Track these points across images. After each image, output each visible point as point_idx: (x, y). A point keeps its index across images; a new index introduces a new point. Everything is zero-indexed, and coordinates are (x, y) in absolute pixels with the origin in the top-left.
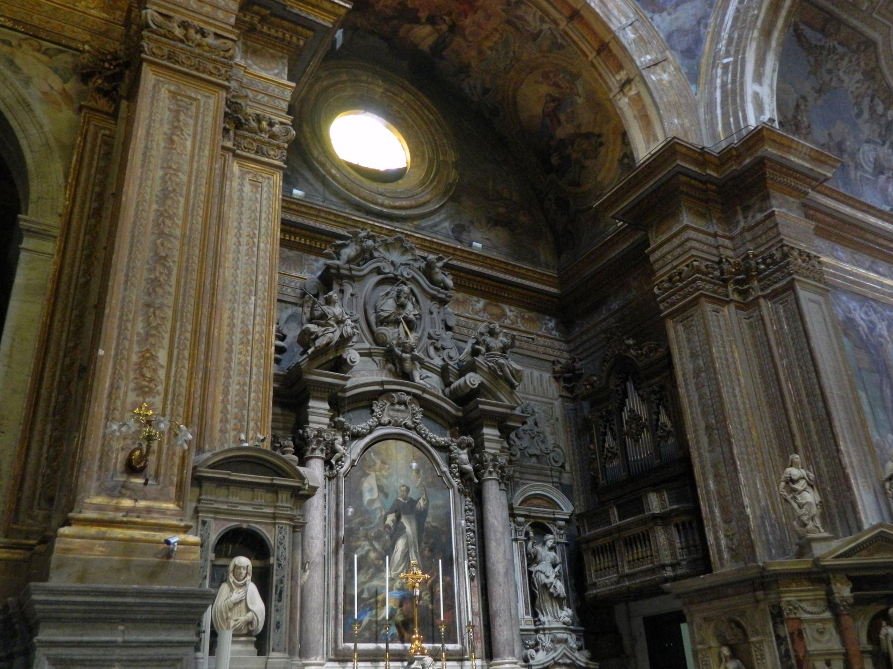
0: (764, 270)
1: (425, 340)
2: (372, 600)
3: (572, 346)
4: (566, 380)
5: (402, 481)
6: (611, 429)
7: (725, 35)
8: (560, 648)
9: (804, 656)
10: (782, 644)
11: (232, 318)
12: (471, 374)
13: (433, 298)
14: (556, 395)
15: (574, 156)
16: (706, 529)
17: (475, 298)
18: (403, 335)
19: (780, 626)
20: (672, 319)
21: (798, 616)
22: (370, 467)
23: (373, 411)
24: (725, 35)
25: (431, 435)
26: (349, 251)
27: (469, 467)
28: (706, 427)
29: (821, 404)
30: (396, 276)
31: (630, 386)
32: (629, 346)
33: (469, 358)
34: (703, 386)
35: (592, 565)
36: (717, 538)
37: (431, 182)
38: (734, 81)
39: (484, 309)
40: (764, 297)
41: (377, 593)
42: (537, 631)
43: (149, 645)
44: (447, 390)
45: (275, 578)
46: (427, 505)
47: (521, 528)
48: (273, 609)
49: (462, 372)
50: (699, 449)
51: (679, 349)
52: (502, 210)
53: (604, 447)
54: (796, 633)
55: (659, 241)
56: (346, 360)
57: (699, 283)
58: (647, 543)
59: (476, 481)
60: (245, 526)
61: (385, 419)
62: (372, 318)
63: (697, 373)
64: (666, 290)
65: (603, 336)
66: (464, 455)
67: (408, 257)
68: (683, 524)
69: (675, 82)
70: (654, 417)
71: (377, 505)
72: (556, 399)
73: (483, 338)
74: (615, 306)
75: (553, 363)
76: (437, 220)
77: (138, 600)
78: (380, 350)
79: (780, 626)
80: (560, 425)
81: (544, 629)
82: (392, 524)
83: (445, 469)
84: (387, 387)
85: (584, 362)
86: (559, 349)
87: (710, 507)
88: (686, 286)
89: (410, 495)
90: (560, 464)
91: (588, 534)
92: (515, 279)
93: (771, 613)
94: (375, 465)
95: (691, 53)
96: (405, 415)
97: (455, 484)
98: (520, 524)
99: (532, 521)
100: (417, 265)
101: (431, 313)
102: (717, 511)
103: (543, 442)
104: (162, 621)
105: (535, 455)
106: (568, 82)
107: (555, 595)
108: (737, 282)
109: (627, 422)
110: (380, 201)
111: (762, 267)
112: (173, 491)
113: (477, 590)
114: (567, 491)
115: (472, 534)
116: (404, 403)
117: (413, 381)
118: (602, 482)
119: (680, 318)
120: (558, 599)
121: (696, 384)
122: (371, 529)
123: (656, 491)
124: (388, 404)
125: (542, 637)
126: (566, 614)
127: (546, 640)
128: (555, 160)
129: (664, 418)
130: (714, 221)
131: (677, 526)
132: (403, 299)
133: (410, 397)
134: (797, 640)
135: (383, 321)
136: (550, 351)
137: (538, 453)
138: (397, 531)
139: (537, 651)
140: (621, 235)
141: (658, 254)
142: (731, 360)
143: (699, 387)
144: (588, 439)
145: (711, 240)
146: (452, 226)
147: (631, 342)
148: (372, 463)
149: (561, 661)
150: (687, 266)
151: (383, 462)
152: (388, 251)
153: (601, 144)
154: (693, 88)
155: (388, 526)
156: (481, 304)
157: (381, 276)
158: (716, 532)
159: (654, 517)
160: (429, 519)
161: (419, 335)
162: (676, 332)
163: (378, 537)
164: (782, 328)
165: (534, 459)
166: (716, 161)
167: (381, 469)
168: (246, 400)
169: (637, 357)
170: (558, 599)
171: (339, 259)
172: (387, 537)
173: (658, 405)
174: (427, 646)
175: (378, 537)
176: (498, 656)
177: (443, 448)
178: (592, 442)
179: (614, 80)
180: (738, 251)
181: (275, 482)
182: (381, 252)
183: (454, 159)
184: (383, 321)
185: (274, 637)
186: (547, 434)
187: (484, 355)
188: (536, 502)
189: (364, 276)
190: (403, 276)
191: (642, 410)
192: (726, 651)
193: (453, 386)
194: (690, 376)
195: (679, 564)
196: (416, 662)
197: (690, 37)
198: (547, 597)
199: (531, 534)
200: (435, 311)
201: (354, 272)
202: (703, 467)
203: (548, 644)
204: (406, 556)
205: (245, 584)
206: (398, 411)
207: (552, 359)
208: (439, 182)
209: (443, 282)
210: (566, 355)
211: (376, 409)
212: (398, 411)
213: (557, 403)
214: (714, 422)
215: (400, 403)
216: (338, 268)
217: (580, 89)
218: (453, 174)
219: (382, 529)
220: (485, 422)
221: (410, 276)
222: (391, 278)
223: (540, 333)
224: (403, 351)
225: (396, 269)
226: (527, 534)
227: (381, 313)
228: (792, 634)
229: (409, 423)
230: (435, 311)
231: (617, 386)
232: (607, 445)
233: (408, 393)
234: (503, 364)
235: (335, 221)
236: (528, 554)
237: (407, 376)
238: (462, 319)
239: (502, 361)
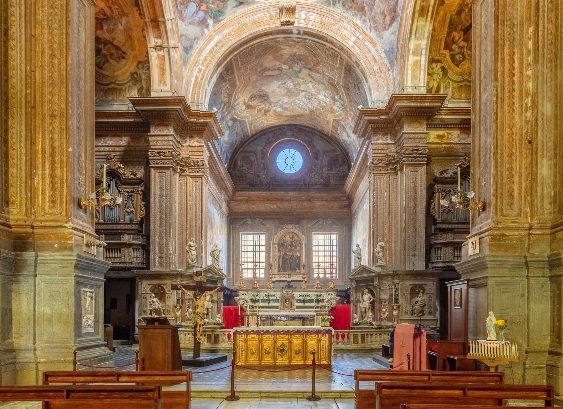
7: (205, 54)
24: (205, 54)
29: (200, 222)
32: (120, 167)
38: (202, 79)
64: (155, 156)
69: (178, 61)
70: (125, 202)
95: (187, 50)
106: (119, 13)
108: (182, 166)
154: (184, 68)
169: (123, 174)
173: (128, 198)
179: (153, 41)
197: (189, 43)
217: (124, 22)
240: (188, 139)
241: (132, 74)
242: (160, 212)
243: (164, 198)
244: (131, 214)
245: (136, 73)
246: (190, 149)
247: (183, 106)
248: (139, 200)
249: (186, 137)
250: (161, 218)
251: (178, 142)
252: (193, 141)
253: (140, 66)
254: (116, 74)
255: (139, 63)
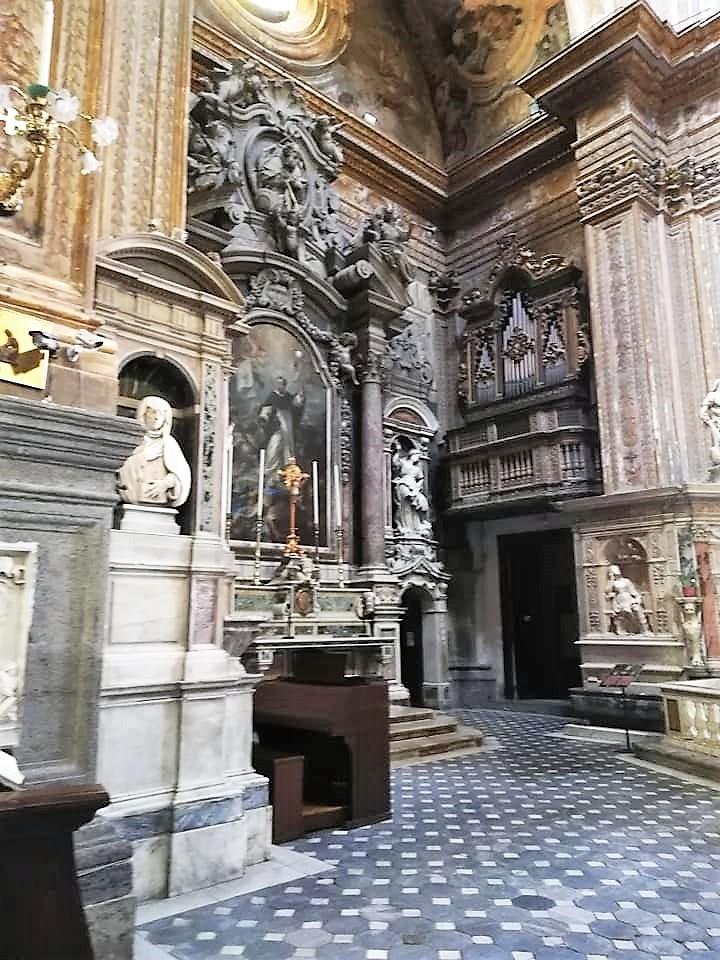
0: (701, 182)
1: (309, 216)
2: (243, 496)
3: (450, 259)
4: (441, 295)
5: (279, 373)
6: (489, 349)
8: (418, 559)
9: (708, 579)
10: (686, 566)
11: (126, 58)
12: (363, 262)
13: (321, 169)
14: (430, 310)
15: (483, 34)
16: (603, 451)
17: (359, 185)
18: (288, 203)
19: (687, 548)
20: (593, 225)
21: (706, 540)
22: (246, 351)
23: (250, 288)
25: (311, 326)
26: (231, 86)
27: (351, 367)
28: (619, 346)
30: (283, 131)
31: (517, 303)
33: (360, 245)
34: (622, 301)
35: (459, 479)
36: (614, 461)
37: (320, 33)
39: (367, 200)
40: (696, 212)
41: (247, 489)
42: (396, 541)
43: (39, 496)
44: (331, 279)
45: (202, 435)
46: (304, 402)
47: (388, 440)
48: (200, 474)
49: (351, 260)
50: (606, 369)
51: (598, 259)
52: (392, 89)
53: (477, 367)
54: (703, 556)
55: (590, 134)
56: (227, 215)
57: (635, 184)
58: (528, 463)
59: (357, 383)
60: (160, 355)
61: (264, 299)
62: (253, 176)
63: (616, 287)
65: (496, 246)
66: (345, 353)
67: (295, 112)
68: (570, 445)
70: (544, 337)
71: (252, 394)
72: (429, 314)
73: (379, 221)
74: (508, 217)
75: (430, 273)
76: (324, 81)
77: (20, 422)
78: (261, 217)
79: (687, 548)
80: (430, 341)
81: (404, 540)
82: (266, 417)
83: (325, 366)
84: (269, 261)
85: (460, 277)
86: (437, 260)
87: (611, 429)
88: (619, 187)
89: (287, 389)
90: (428, 381)
91: (458, 451)
92: (404, 170)
93: (679, 536)
94: (251, 349)
96: (286, 298)
97: (335, 386)
98: (387, 436)
99: (399, 434)
100: (307, 123)
101: (317, 187)
102: (618, 433)
103: (414, 355)
104: (60, 462)
105: (407, 368)
107: (418, 508)
109: (509, 341)
110: (262, 39)
111: (700, 177)
112: (66, 263)
113: (349, 497)
114: (433, 407)
115: (347, 439)
116: (286, 284)
117: (297, 259)
118: (470, 402)
119: (604, 224)
120: (421, 513)
121: (613, 299)
122: (244, 420)
123: (545, 411)
124: (268, 282)
125: (401, 546)
126: (425, 527)
127: (404, 550)
128: (458, 38)
129: (554, 338)
130: (653, 120)
131: (563, 446)
132: (291, 159)
133: (292, 278)
134: (703, 563)
135: (267, 182)
136: (427, 260)
137: (410, 366)
138: (272, 426)
139: (396, 559)
140: (534, 129)
141: (587, 149)
142: (654, 277)
143: (615, 302)
144: (458, 359)
145: (648, 139)
146: (339, 94)
147: (528, 254)
148: (247, 347)
149: (418, 571)
150: (624, 164)
151: (260, 349)
152: (274, 97)
153: (519, 22)
155: (263, 419)
156: (365, 193)
157: (265, 128)
158: (613, 455)
159: (542, 436)
160: (306, 417)
161: (305, 207)
162: (596, 241)
163: (252, 430)
164: (711, 247)
165: (404, 372)
166: (673, 41)
167: (256, 356)
168: (149, 186)
169: (533, 271)
170: (421, 513)
171: (216, 93)
172: (262, 431)
173: (550, 324)
174: (304, 548)
175: (252, 430)
176: (368, 562)
177: (326, 344)
178: (464, 361)
180: (672, 158)
181: (203, 299)
182: (266, 96)
183: (346, 12)
184: (267, 182)
185: (201, 512)
186: (419, 349)
187: (377, 241)
188: (404, 416)
189: (246, 121)
190: (289, 133)
191: (530, 331)
192: (615, 569)
193: (338, 275)
194: (607, 289)
195: (560, 484)
196: (291, 563)
198: (408, 509)
199: (399, 447)
200: (322, 185)
201: (234, 114)
202: (608, 387)
203: (407, 554)
204: (280, 453)
205: (161, 436)
206: (279, 292)
207: (430, 269)
208: (329, 33)
209: (333, 152)
210: (443, 269)
211: (254, 285)
212: (279, 292)
213: (431, 317)
214: (630, 340)
215: (280, 283)
216: (215, 103)
218: (345, 28)
219: (255, 421)
220: (372, 320)
221: (296, 136)
222: (275, 132)
223: (420, 238)
224: (289, 223)
225: (283, 123)
226: (393, 446)
227: (266, 172)
228: (699, 557)
229: (289, 309)
230: (322, 185)
231: (503, 303)
232: (481, 366)
233: (292, 273)
234: (398, 254)
235: (213, 45)
236: (393, 466)
237: (292, 253)
238: (345, 205)
239: (397, 251)
240: (681, 119)
241: (539, 46)
242: (617, 330)
243: (624, 289)
244: (559, 362)
245: (546, 39)
246: (690, 141)
247: (645, 26)
248: (575, 321)
249: (675, 116)
250: (622, 347)
251: (653, 136)
252: (695, 117)
253: (553, 18)
254: (508, 67)
255: (549, 12)
